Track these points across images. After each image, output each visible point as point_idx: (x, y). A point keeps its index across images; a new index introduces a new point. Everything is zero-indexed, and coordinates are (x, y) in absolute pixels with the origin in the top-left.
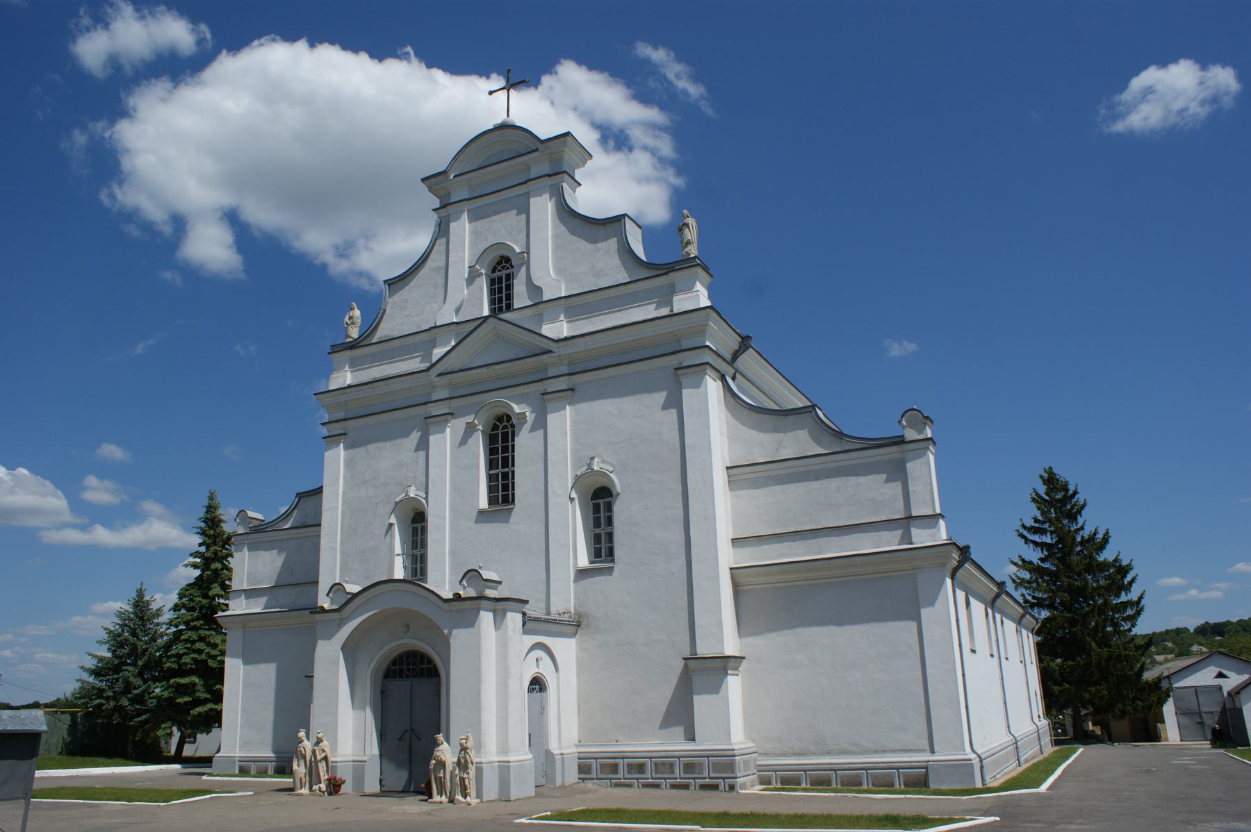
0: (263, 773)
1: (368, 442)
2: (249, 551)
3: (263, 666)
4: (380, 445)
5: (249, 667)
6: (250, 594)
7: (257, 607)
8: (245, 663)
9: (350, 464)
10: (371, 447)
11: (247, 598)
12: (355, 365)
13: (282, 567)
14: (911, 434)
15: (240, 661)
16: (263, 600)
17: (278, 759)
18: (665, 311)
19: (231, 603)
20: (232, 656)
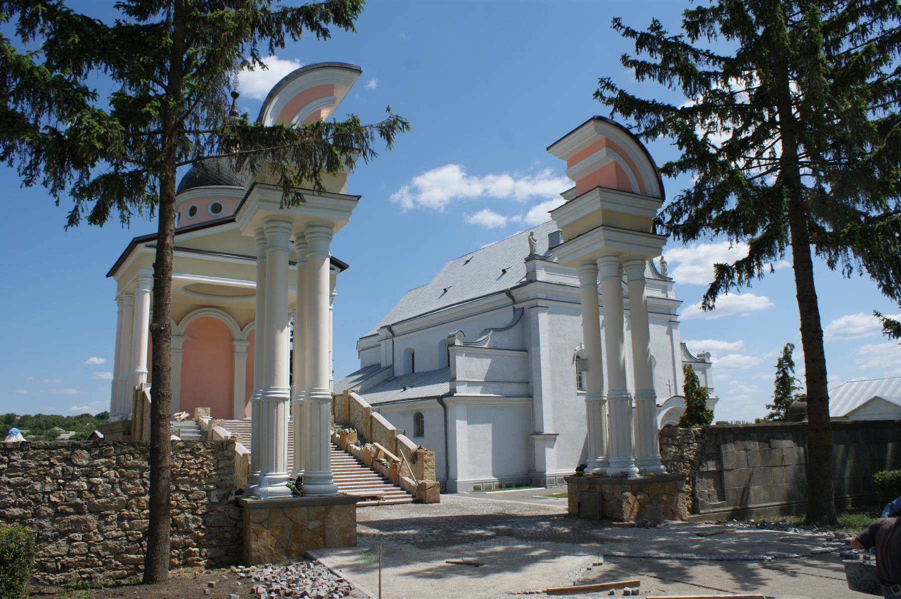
0: (489, 488)
1: (559, 314)
2: (466, 356)
3: (485, 425)
4: (565, 316)
5: (469, 426)
6: (470, 384)
7: (476, 392)
8: (468, 424)
9: (551, 324)
10: (561, 316)
11: (468, 386)
12: (547, 269)
13: (489, 370)
14: (707, 361)
15: (466, 422)
16: (480, 388)
17: (500, 480)
18: (663, 296)
19: (457, 388)
20: (460, 419)
